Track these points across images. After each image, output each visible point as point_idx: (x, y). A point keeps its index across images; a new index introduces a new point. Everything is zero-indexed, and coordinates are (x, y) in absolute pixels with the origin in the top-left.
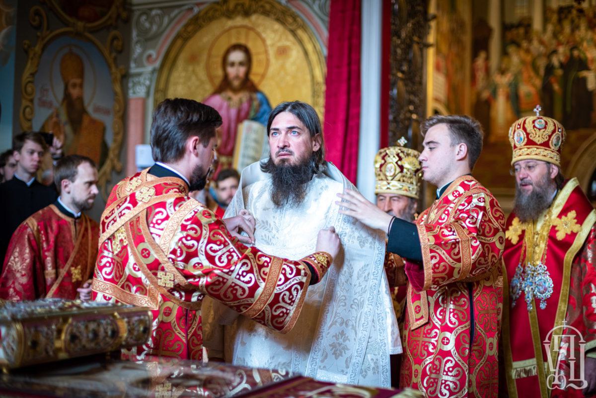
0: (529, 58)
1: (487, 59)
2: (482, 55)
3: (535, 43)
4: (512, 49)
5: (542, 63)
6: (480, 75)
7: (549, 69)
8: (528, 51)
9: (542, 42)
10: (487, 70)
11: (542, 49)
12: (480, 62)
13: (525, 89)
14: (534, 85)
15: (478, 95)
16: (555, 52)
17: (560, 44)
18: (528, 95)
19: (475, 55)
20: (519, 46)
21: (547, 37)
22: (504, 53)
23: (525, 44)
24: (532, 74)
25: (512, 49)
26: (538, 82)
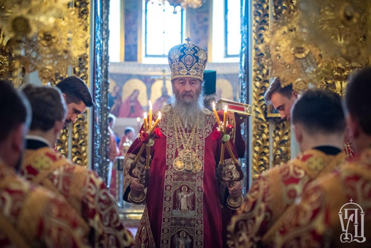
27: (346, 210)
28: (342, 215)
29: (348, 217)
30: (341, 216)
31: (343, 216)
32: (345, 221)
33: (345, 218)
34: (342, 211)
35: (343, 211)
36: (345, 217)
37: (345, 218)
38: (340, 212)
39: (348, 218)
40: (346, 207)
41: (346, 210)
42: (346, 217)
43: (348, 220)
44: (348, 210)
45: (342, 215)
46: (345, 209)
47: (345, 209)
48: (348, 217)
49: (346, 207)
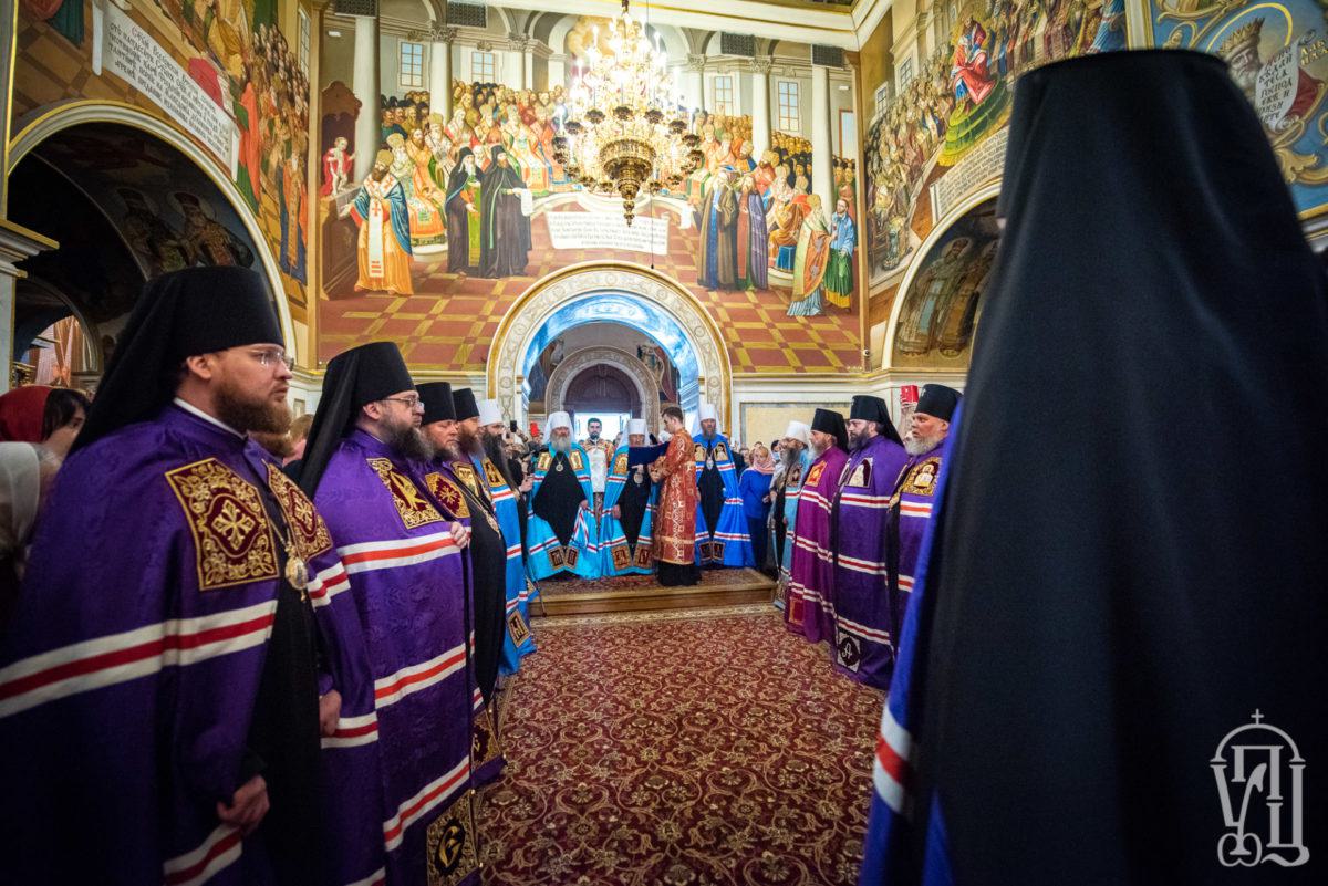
0: (424, 157)
1: (350, 150)
2: (342, 143)
3: (435, 135)
4: (394, 139)
5: (446, 165)
6: (338, 175)
7: (459, 178)
8: (422, 145)
9: (446, 135)
10: (350, 169)
11: (446, 145)
12: (337, 152)
13: (416, 206)
14: (433, 201)
15: (333, 208)
16: (467, 151)
17: (475, 140)
18: (424, 215)
19: (326, 144)
20: (406, 136)
21: (455, 127)
22: (381, 144)
23: (417, 134)
24: (431, 184)
25: (394, 139)
26: (441, 197)
27: (1239, 751)
28: (1225, 766)
29: (1247, 774)
30: (1219, 772)
31: (1229, 773)
32: (1236, 791)
33: (1233, 780)
34: (1223, 755)
35: (1229, 755)
36: (1225, 770)
37: (1233, 780)
38: (1218, 758)
39: (1243, 780)
40: (1237, 740)
41: (1239, 751)
42: (1239, 777)
43: (1243, 785)
44: (1245, 751)
45: (1225, 766)
46: (1233, 747)
47: (1233, 747)
48: (1247, 774)
49: (1237, 740)
